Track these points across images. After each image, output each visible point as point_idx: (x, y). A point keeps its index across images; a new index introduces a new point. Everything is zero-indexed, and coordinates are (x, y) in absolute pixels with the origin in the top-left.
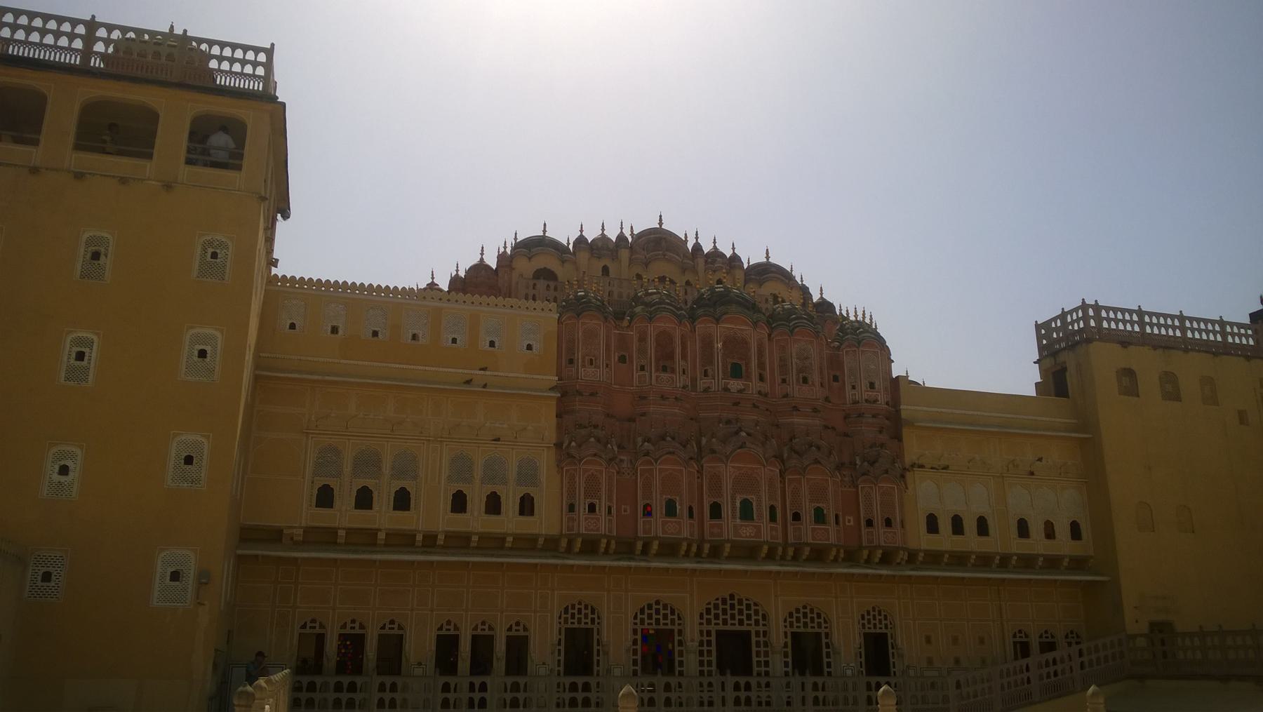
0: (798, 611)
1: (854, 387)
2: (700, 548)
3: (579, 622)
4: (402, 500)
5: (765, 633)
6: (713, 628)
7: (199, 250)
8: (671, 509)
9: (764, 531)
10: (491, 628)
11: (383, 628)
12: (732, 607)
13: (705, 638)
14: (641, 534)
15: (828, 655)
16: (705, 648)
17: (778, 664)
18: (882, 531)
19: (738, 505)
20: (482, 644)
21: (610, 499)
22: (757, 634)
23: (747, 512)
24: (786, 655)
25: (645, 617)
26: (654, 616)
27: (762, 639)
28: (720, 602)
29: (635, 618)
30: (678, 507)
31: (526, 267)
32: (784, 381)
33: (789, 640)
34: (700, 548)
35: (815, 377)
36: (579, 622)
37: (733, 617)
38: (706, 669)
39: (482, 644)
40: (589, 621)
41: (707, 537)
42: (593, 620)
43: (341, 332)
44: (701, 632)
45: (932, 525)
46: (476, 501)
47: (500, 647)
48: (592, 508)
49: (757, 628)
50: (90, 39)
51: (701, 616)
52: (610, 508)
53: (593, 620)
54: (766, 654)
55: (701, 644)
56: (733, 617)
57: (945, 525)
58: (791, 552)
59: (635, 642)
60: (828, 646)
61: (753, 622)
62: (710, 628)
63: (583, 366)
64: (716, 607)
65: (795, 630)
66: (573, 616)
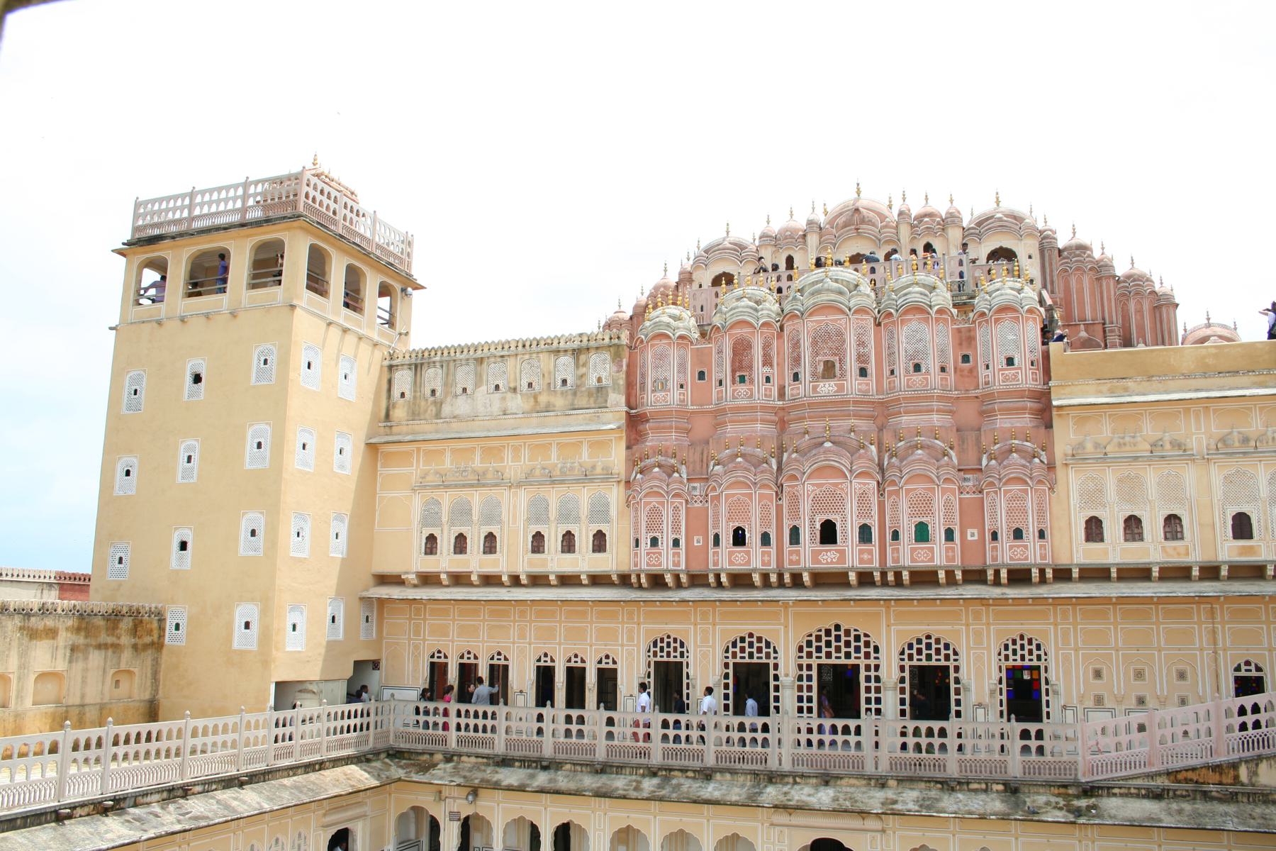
0: (919, 641)
1: (988, 367)
2: (781, 576)
3: (668, 654)
4: (490, 543)
5: (877, 667)
6: (814, 662)
7: (255, 361)
8: (739, 538)
9: (849, 554)
10: (583, 661)
11: (492, 658)
12: (838, 638)
13: (805, 673)
14: (711, 567)
15: (958, 692)
16: (805, 683)
17: (891, 702)
18: (1006, 546)
19: (818, 527)
20: (576, 677)
21: (676, 528)
22: (868, 668)
23: (828, 533)
24: (902, 691)
25: (738, 650)
26: (748, 650)
27: (873, 673)
28: (823, 633)
29: (727, 651)
30: (747, 535)
31: (706, 277)
32: (892, 372)
33: (907, 674)
34: (781, 576)
35: (931, 364)
36: (668, 654)
37: (838, 649)
38: (805, 705)
39: (576, 677)
40: (678, 654)
41: (786, 565)
42: (682, 653)
43: (438, 394)
44: (800, 667)
45: (1094, 529)
46: (553, 541)
47: (591, 679)
48: (654, 542)
49: (867, 662)
50: (191, 207)
51: (801, 649)
52: (676, 543)
53: (682, 654)
54: (878, 690)
55: (800, 678)
56: (838, 649)
57: (1113, 529)
58: (891, 577)
59: (726, 676)
60: (957, 681)
61: (862, 655)
62: (809, 661)
63: (653, 391)
64: (819, 639)
65: (915, 663)
66: (662, 649)
